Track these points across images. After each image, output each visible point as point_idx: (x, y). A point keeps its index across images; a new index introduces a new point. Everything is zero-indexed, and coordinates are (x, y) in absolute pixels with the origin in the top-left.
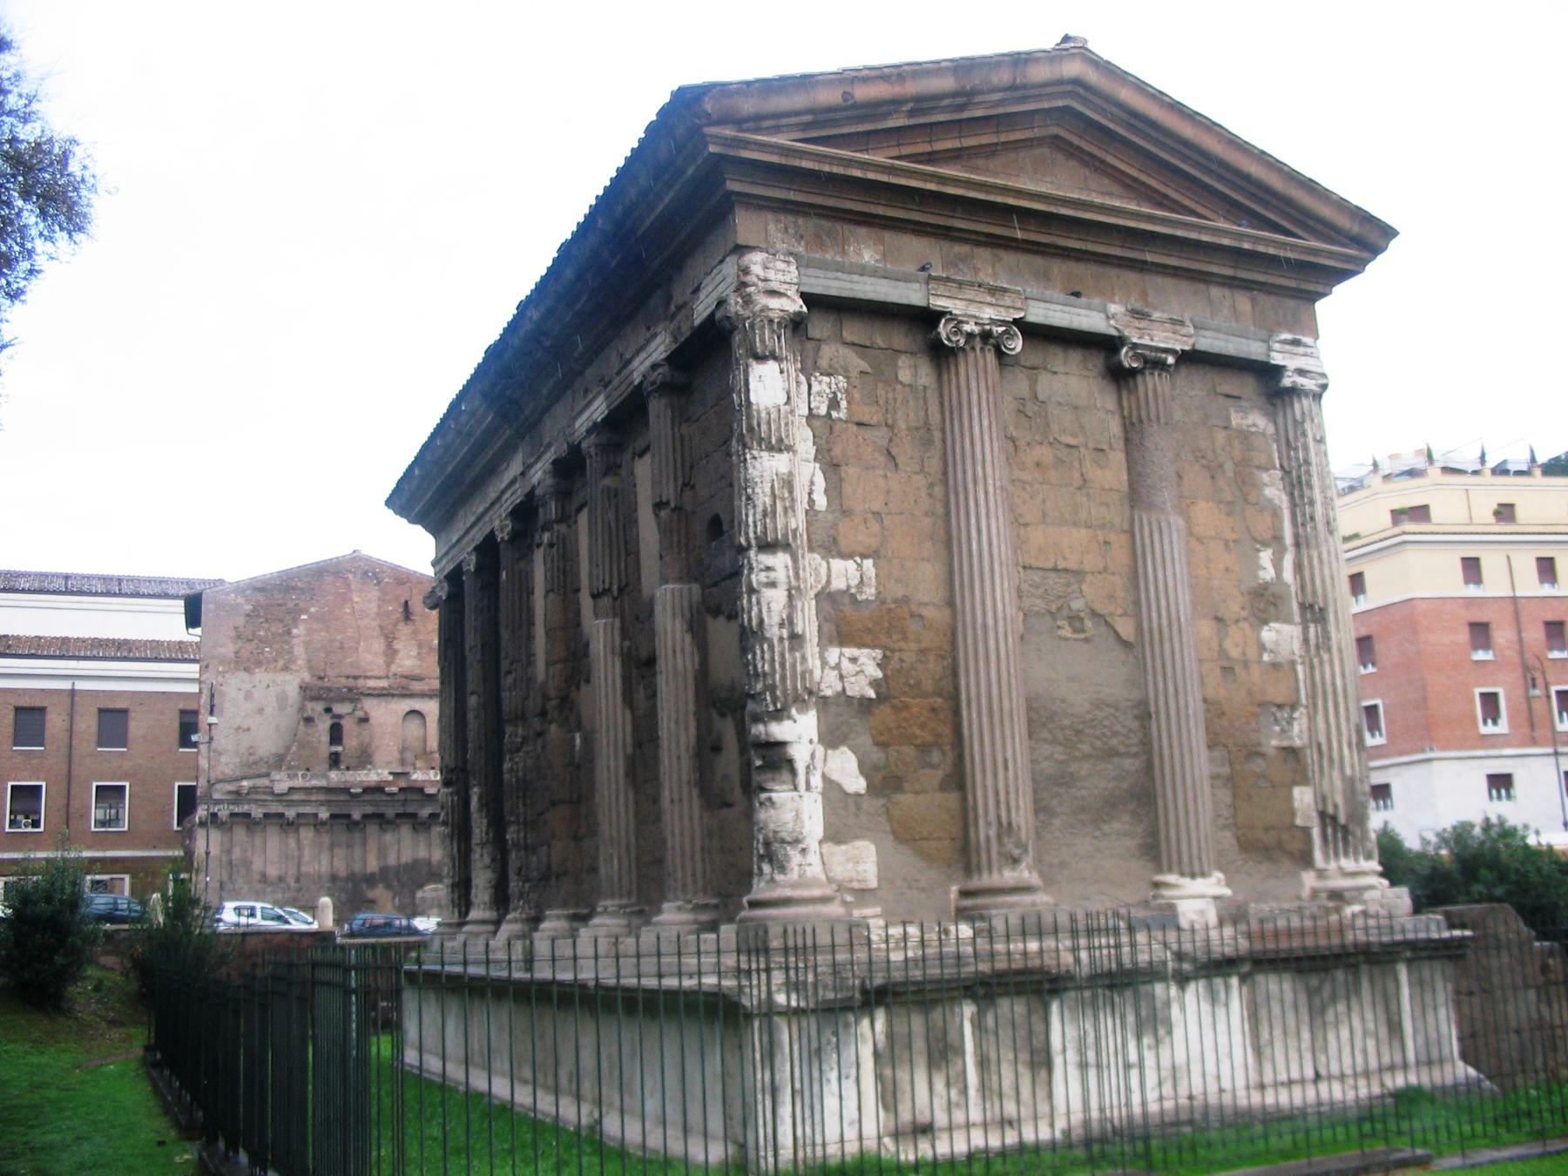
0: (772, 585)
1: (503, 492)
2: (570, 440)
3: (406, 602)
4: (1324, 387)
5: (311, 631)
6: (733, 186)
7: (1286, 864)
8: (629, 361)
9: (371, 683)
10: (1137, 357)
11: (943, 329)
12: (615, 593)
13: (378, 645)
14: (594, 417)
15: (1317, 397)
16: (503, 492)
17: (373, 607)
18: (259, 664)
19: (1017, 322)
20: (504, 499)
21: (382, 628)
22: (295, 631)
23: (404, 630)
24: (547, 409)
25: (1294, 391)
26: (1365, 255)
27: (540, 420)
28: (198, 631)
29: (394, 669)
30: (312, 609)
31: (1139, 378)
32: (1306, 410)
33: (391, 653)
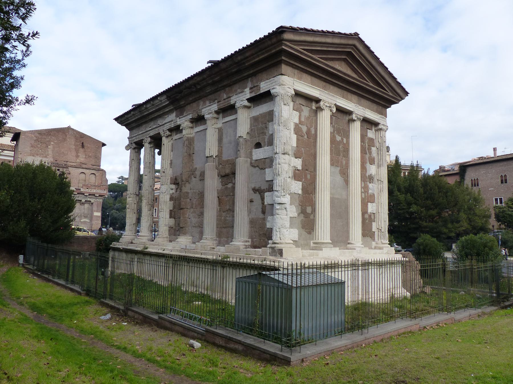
0: (285, 163)
1: (166, 123)
2: (199, 114)
3: (83, 143)
4: (387, 129)
5: (54, 147)
6: (283, 58)
7: (369, 239)
8: (230, 97)
9: (71, 164)
10: (356, 117)
11: (322, 103)
12: (214, 157)
13: (74, 153)
14: (211, 109)
15: (386, 131)
16: (166, 123)
17: (73, 143)
18: (37, 155)
19: (335, 105)
20: (165, 125)
21: (75, 149)
22: (49, 147)
23: (81, 150)
24: (189, 104)
25: (381, 129)
26: (400, 99)
27: (185, 106)
28: (15, 142)
29: (78, 161)
30: (55, 141)
31: (355, 122)
32: (383, 134)
33: (77, 156)
